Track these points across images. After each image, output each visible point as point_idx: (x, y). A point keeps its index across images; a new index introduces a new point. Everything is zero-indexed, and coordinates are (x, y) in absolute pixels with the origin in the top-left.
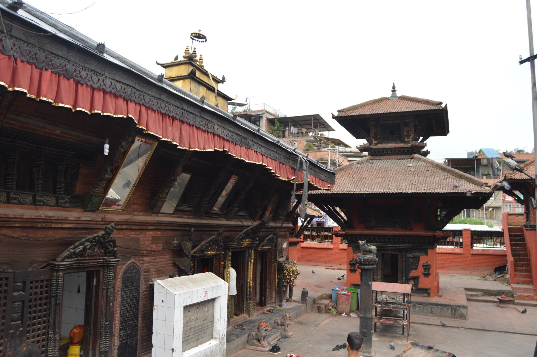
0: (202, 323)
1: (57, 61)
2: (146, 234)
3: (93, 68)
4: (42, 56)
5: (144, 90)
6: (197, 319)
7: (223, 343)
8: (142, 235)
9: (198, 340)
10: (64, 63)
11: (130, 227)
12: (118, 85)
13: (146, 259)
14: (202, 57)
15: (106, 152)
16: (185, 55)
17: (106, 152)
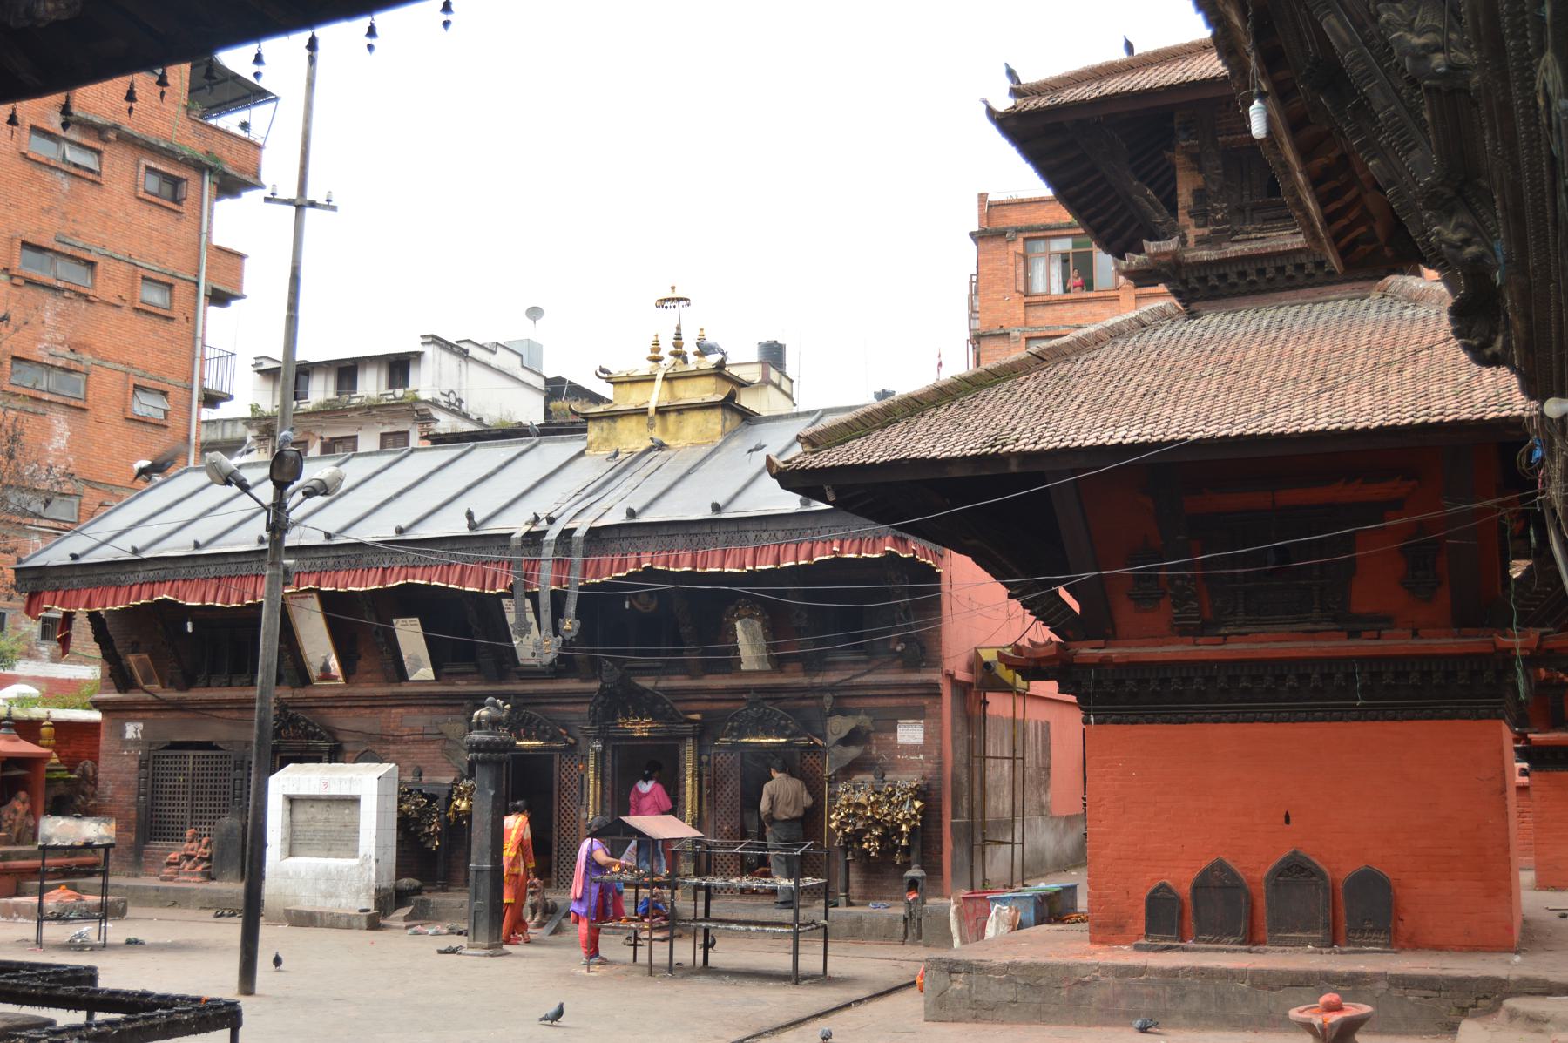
0: (338, 828)
1: (104, 578)
2: (390, 713)
3: (128, 569)
4: (94, 579)
5: (178, 565)
6: (327, 820)
7: (366, 866)
8: (383, 715)
9: (329, 850)
10: (107, 576)
11: (356, 703)
12: (151, 573)
13: (392, 747)
14: (704, 333)
15: (190, 629)
16: (652, 355)
17: (190, 629)
